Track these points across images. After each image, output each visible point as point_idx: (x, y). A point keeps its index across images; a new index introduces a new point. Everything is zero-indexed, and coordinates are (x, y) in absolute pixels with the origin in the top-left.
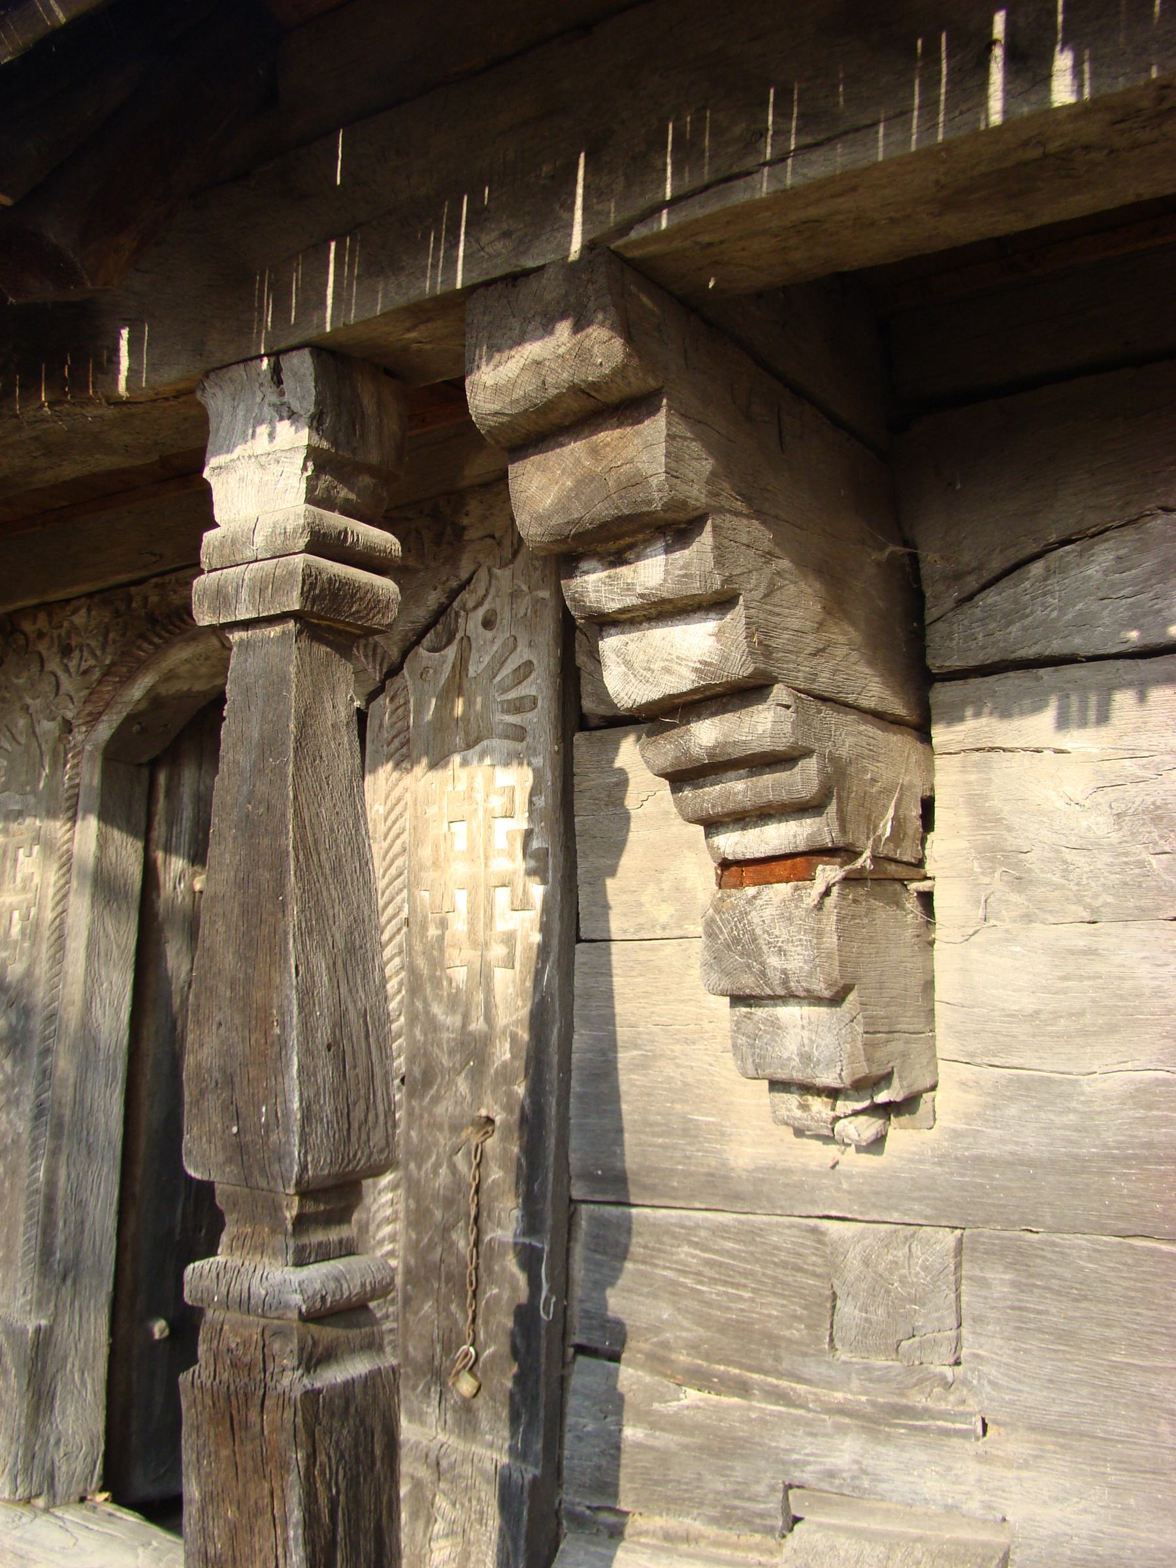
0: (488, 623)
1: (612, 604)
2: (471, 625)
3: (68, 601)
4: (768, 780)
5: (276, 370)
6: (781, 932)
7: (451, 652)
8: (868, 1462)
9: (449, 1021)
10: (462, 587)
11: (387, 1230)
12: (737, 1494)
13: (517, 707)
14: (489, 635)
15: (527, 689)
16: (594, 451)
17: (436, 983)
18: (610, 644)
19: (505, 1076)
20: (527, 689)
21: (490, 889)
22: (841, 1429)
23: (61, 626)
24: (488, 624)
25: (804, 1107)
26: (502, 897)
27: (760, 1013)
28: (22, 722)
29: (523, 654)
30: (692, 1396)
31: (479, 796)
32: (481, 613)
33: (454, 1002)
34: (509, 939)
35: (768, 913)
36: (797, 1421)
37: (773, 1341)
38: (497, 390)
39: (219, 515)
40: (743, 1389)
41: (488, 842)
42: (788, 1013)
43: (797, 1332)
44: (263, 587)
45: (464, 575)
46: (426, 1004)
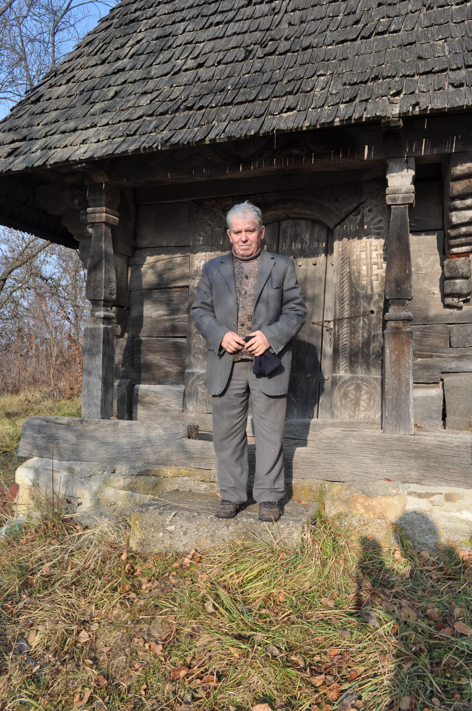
0: (370, 211)
1: (460, 206)
2: (364, 211)
3: (224, 198)
4: (469, 238)
5: (407, 160)
6: (463, 266)
7: (359, 217)
8: (459, 365)
9: (362, 292)
10: (363, 203)
11: (345, 336)
12: (431, 375)
13: (380, 228)
14: (370, 213)
15: (381, 225)
16: (470, 182)
17: (358, 285)
18: (454, 213)
19: (377, 302)
20: (381, 225)
21: (371, 265)
22: (453, 361)
23: (221, 204)
24: (370, 211)
25: (453, 300)
26: (375, 267)
27: (452, 281)
28: (208, 228)
29: (379, 218)
30: (419, 359)
31: (368, 246)
32: (367, 209)
33: (363, 288)
34: (377, 275)
35: (460, 262)
36: (443, 360)
37: (437, 347)
38: (461, 171)
39: (389, 184)
40: (431, 356)
41: (371, 255)
42: (458, 281)
43: (443, 345)
44: (404, 198)
45: (363, 200)
46: (355, 289)
